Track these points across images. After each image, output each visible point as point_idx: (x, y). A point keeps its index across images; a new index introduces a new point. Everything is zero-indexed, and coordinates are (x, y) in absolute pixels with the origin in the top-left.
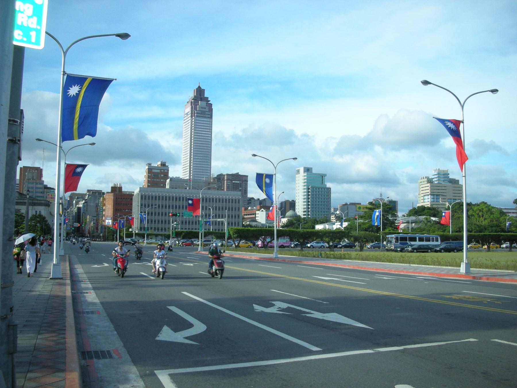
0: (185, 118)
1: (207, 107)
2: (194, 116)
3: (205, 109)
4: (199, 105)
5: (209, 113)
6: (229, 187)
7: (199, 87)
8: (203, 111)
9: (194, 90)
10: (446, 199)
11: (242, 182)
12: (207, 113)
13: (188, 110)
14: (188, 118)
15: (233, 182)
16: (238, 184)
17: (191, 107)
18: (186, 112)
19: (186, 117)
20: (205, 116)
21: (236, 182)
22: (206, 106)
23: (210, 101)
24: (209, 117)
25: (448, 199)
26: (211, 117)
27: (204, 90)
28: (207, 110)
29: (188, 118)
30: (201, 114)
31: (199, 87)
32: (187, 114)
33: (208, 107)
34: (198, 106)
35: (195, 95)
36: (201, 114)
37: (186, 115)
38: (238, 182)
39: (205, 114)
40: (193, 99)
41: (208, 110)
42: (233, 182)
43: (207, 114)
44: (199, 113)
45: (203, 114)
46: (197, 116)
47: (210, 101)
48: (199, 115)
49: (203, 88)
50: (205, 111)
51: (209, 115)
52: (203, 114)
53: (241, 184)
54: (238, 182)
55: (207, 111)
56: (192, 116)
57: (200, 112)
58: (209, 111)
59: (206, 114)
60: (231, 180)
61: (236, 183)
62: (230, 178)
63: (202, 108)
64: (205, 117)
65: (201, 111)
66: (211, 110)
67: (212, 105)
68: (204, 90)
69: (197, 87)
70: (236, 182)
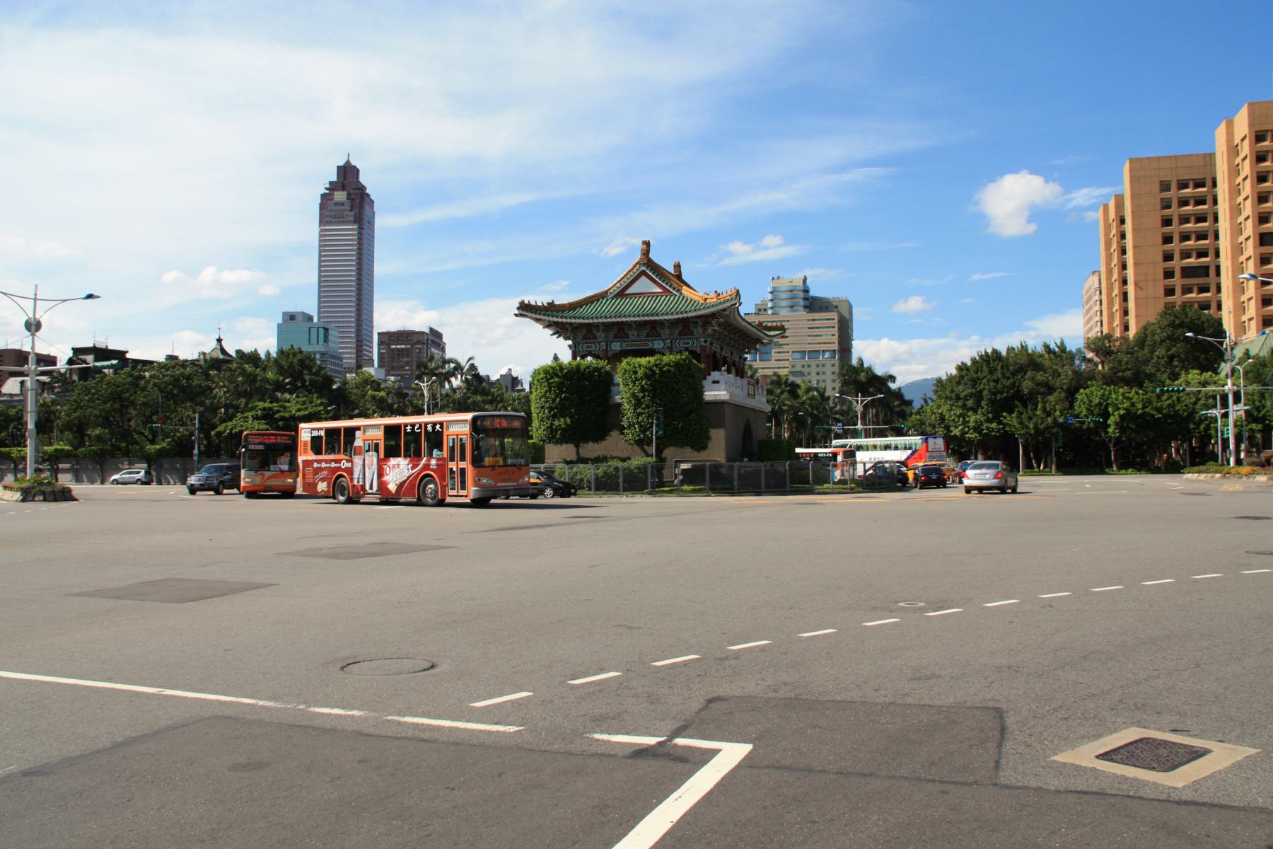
5: (352, 213)
8: (339, 210)
10: (788, 352)
15: (393, 347)
16: (403, 350)
20: (343, 219)
21: (398, 347)
22: (348, 199)
24: (350, 221)
25: (793, 352)
28: (347, 207)
30: (335, 217)
31: (348, 162)
33: (349, 201)
38: (403, 346)
41: (349, 208)
42: (393, 347)
43: (347, 216)
44: (331, 216)
49: (353, 163)
50: (344, 210)
53: (407, 350)
54: (403, 346)
55: (347, 210)
57: (332, 213)
58: (351, 211)
60: (387, 344)
61: (398, 350)
62: (386, 339)
63: (336, 204)
64: (343, 222)
65: (335, 210)
69: (342, 164)
70: (398, 347)
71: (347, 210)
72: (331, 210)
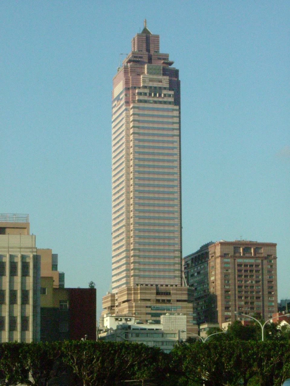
0: (115, 110)
1: (165, 77)
2: (134, 102)
3: (161, 81)
4: (143, 73)
5: (172, 93)
6: (229, 274)
7: (145, 31)
8: (155, 88)
9: (134, 39)
11: (262, 261)
12: (165, 92)
13: (119, 88)
14: (120, 108)
17: (126, 79)
18: (116, 95)
19: (115, 105)
20: (160, 99)
23: (171, 64)
24: (170, 103)
26: (177, 101)
27: (157, 37)
29: (120, 108)
31: (145, 31)
32: (118, 99)
33: (167, 78)
34: (142, 76)
35: (135, 51)
36: (150, 95)
37: (116, 102)
39: (160, 95)
40: (129, 61)
41: (167, 86)
44: (145, 94)
45: (155, 95)
46: (140, 101)
47: (171, 64)
48: (146, 98)
49: (153, 31)
50: (160, 88)
51: (170, 96)
52: (155, 95)
55: (165, 88)
56: (127, 103)
57: (147, 91)
58: (170, 89)
59: (163, 95)
62: (230, 250)
65: (150, 87)
66: (175, 86)
67: (175, 73)
68: (157, 37)
69: (140, 31)
71: (165, 88)
72: (145, 87)
